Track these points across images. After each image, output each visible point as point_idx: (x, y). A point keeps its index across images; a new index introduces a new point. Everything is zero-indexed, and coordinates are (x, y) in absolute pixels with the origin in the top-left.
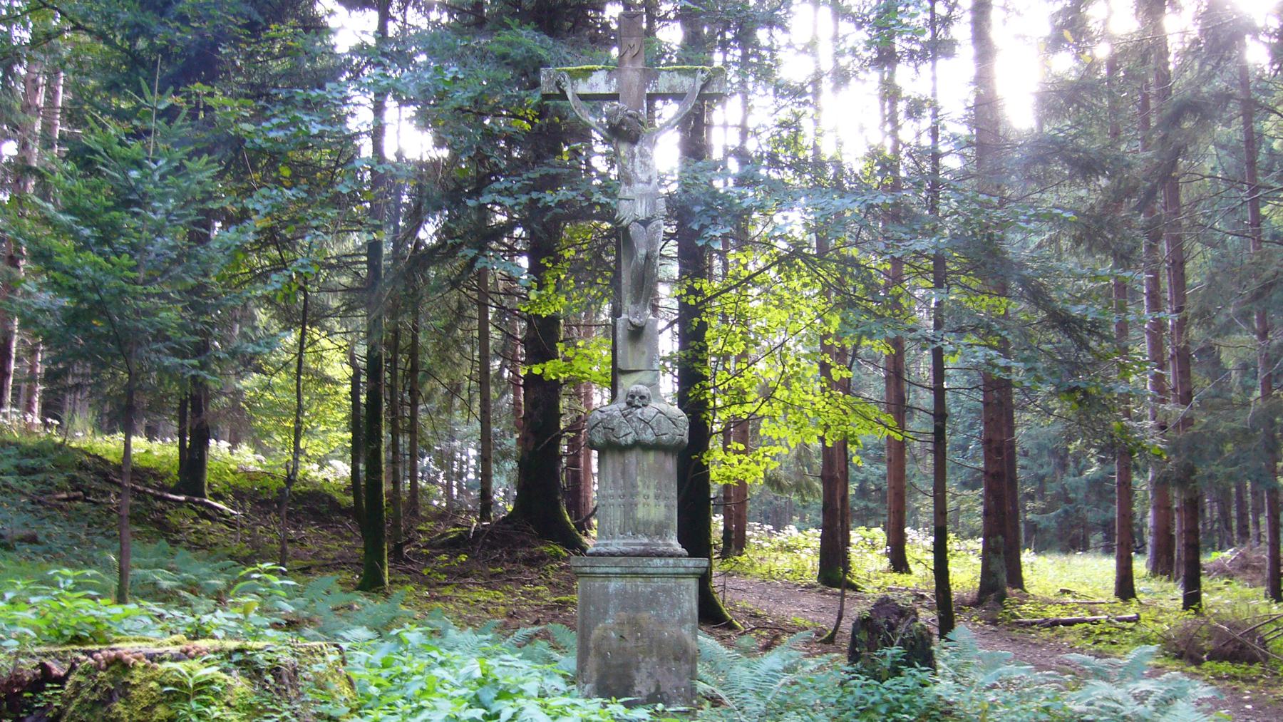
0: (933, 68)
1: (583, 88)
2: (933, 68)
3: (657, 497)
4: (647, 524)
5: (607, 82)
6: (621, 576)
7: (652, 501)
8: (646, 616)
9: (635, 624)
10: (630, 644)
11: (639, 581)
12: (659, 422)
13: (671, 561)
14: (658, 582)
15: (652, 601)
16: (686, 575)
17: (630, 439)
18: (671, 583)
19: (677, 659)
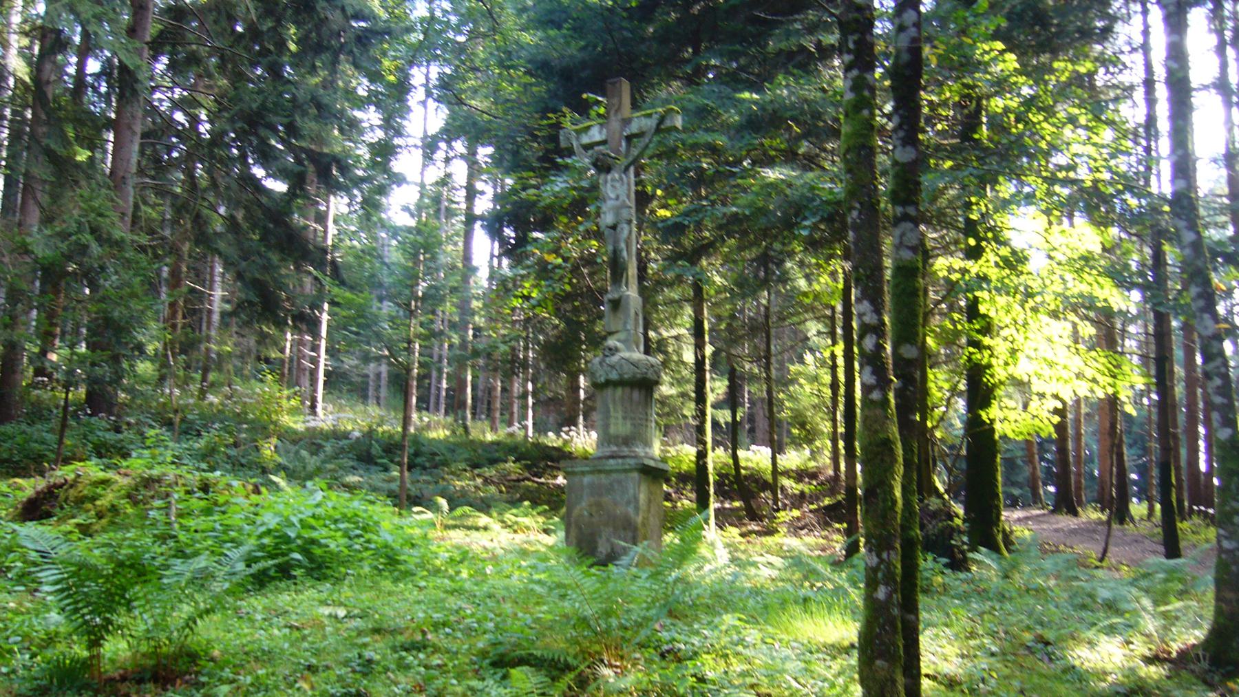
0: (425, 131)
1: (585, 140)
2: (425, 131)
3: (624, 418)
4: (617, 437)
5: (600, 133)
6: (591, 472)
7: (620, 421)
8: (606, 500)
9: (599, 505)
10: (595, 519)
11: (603, 476)
12: (621, 366)
13: (620, 461)
14: (614, 476)
15: (610, 489)
16: (631, 470)
17: (603, 379)
18: (622, 476)
19: (625, 529)
